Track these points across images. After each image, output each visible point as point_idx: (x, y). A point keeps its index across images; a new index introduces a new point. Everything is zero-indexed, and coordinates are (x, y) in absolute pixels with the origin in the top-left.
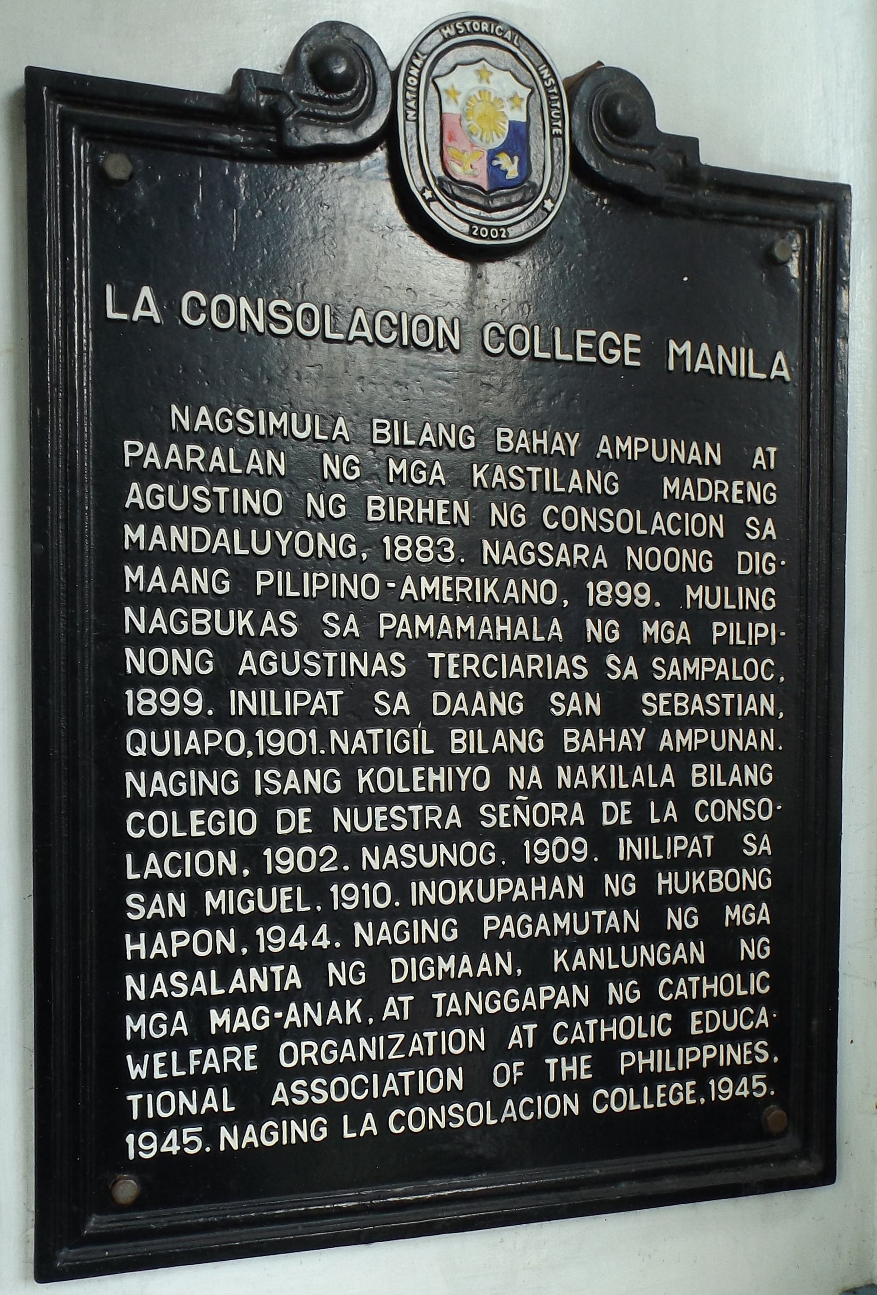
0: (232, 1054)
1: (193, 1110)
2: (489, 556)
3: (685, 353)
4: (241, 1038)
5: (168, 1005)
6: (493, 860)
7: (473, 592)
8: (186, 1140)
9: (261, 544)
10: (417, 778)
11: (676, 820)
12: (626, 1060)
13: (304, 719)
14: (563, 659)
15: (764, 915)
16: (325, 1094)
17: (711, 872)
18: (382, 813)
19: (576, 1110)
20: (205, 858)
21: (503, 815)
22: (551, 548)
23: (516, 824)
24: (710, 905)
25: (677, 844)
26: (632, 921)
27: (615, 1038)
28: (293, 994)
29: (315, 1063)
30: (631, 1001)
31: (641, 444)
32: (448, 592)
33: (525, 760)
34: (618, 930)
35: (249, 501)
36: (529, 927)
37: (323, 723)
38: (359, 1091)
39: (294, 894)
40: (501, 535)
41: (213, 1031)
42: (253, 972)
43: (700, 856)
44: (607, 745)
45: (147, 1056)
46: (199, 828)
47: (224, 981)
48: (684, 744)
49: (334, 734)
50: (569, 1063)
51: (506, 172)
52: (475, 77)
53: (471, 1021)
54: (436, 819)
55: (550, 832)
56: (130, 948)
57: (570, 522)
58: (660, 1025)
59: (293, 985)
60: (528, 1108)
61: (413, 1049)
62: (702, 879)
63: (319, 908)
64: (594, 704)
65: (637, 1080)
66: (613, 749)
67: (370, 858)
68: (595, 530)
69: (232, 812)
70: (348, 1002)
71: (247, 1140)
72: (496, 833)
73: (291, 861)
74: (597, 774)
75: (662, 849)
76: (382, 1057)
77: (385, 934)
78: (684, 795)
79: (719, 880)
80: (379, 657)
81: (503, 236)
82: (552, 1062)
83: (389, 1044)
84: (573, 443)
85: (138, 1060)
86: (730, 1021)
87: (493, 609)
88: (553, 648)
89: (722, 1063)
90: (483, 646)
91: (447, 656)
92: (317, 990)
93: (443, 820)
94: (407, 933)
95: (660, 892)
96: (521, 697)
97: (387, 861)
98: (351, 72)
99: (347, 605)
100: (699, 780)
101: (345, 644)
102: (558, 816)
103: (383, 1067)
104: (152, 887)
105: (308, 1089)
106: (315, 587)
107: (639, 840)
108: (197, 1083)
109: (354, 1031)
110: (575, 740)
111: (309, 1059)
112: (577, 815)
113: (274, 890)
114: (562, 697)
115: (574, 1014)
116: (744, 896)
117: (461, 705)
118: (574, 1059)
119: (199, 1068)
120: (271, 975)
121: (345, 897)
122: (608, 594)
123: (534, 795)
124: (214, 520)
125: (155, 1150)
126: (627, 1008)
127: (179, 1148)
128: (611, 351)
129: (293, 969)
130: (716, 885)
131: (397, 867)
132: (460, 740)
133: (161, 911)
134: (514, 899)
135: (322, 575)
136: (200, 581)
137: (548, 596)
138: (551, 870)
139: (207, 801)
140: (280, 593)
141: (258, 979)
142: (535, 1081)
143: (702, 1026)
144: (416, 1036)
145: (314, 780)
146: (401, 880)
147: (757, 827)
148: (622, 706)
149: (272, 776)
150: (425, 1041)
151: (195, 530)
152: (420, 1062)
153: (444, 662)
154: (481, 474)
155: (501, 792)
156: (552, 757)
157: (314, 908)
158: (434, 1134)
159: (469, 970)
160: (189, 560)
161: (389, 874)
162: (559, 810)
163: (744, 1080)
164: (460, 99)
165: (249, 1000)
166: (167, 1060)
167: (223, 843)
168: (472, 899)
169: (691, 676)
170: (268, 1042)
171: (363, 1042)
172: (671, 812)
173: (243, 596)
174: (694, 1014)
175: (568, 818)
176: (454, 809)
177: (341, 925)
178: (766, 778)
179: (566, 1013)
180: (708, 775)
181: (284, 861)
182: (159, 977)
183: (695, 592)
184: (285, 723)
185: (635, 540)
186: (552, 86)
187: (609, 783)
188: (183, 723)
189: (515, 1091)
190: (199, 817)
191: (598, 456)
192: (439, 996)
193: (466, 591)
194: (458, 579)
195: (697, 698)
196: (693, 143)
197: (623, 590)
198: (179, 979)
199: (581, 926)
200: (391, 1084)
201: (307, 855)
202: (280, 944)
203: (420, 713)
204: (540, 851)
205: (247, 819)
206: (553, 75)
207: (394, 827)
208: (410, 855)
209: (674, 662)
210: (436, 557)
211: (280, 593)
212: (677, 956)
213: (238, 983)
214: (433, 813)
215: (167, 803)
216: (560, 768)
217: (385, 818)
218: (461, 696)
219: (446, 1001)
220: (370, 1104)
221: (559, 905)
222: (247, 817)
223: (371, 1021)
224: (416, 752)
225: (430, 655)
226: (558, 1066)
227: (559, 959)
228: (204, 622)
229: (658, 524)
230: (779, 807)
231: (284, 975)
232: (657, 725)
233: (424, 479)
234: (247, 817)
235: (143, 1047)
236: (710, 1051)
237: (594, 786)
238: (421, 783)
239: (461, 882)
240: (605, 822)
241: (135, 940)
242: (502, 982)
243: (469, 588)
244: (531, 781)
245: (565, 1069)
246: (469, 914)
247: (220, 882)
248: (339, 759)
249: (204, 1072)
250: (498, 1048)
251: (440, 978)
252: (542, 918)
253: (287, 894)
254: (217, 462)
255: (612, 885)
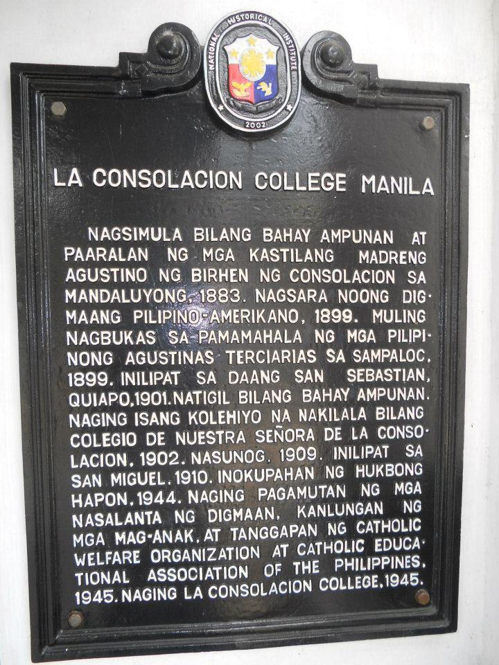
0: (127, 555)
2: (260, 298)
4: (132, 547)
5: (95, 530)
7: (250, 317)
9: (136, 297)
10: (220, 417)
11: (367, 438)
12: (339, 563)
14: (302, 352)
16: (175, 576)
17: (387, 465)
18: (202, 435)
21: (268, 436)
22: (295, 293)
24: (387, 483)
25: (368, 450)
27: (332, 552)
33: (282, 406)
34: (334, 496)
35: (129, 275)
36: (284, 494)
37: (169, 389)
39: (156, 475)
40: (266, 286)
41: (117, 543)
44: (327, 398)
45: (84, 555)
46: (107, 442)
47: (122, 518)
49: (175, 394)
50: (306, 564)
51: (265, 92)
55: (296, 444)
56: (74, 501)
57: (306, 277)
58: (358, 546)
61: (221, 556)
65: (345, 574)
70: (186, 531)
71: (135, 597)
73: (154, 459)
75: (358, 453)
76: (204, 560)
78: (372, 424)
79: (391, 470)
80: (199, 354)
81: (264, 126)
82: (297, 564)
83: (208, 554)
84: (306, 235)
86: (397, 544)
87: (261, 326)
88: (296, 346)
89: (392, 567)
90: (257, 346)
92: (169, 524)
93: (235, 439)
95: (357, 476)
96: (278, 373)
97: (205, 460)
100: (380, 416)
101: (181, 347)
103: (205, 565)
104: (84, 471)
105: (166, 573)
106: (165, 318)
108: (111, 568)
109: (190, 546)
111: (166, 559)
112: (311, 435)
114: (302, 372)
115: (310, 540)
116: (405, 479)
117: (244, 378)
118: (309, 562)
119: (110, 561)
120: (146, 517)
122: (327, 316)
123: (286, 424)
124: (111, 286)
126: (339, 537)
128: (328, 184)
129: (157, 513)
133: (89, 483)
136: (105, 317)
138: (295, 465)
139: (111, 429)
141: (139, 518)
142: (288, 573)
144: (222, 550)
145: (165, 418)
147: (414, 441)
148: (336, 376)
149: (144, 416)
151: (102, 291)
153: (235, 356)
154: (254, 254)
155: (267, 424)
157: (167, 483)
159: (250, 516)
160: (99, 307)
161: (206, 466)
163: (406, 576)
165: (136, 528)
166: (95, 557)
167: (120, 450)
168: (252, 480)
170: (146, 549)
173: (127, 324)
175: (305, 437)
177: (181, 491)
179: (303, 538)
180: (386, 413)
182: (89, 516)
184: (150, 389)
185: (343, 286)
186: (291, 44)
187: (328, 418)
188: (98, 389)
189: (276, 579)
190: (107, 437)
192: (234, 530)
194: (242, 311)
196: (374, 68)
199: (313, 493)
204: (291, 455)
207: (208, 442)
208: (217, 457)
210: (229, 299)
212: (367, 510)
213: (129, 519)
216: (301, 411)
218: (245, 373)
219: (238, 533)
220: (198, 582)
225: (227, 352)
226: (300, 567)
227: (300, 511)
228: (107, 338)
229: (357, 277)
231: (152, 516)
232: (356, 387)
233: (222, 259)
235: (82, 550)
237: (320, 420)
238: (222, 420)
240: (326, 439)
241: (77, 498)
242: (269, 523)
243: (249, 315)
244: (284, 418)
245: (304, 568)
246: (250, 489)
247: (118, 469)
248: (178, 407)
249: (113, 563)
250: (267, 556)
251: (235, 520)
252: (291, 489)
255: (330, 472)
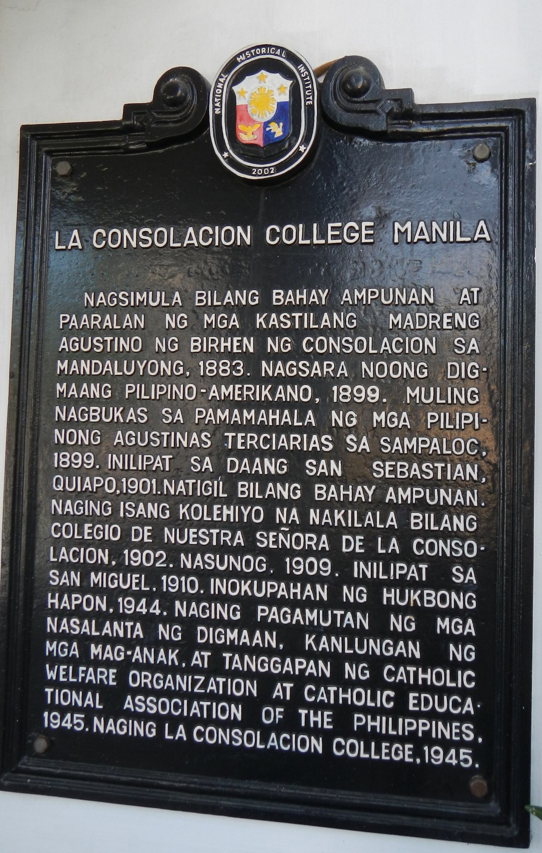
0: (102, 673)
1: (80, 703)
2: (266, 371)
3: (407, 230)
4: (108, 664)
5: (69, 638)
6: (264, 569)
7: (254, 394)
8: (75, 721)
9: (129, 369)
10: (216, 512)
11: (398, 552)
12: (359, 720)
13: (148, 472)
14: (315, 437)
15: (470, 628)
16: (154, 707)
17: (426, 592)
18: (194, 533)
19: (320, 750)
20: (91, 553)
21: (271, 539)
22: (308, 365)
23: (280, 547)
24: (426, 617)
25: (399, 569)
26: (363, 621)
27: (349, 702)
28: (138, 641)
29: (150, 686)
30: (362, 678)
31: (373, 293)
32: (239, 395)
33: (288, 504)
34: (353, 626)
35: (123, 343)
36: (289, 616)
37: (158, 475)
38: (176, 709)
39: (140, 578)
40: (274, 357)
41: (92, 657)
42: (116, 624)
43: (417, 579)
44: (346, 496)
45: (56, 667)
46: (89, 534)
47: (99, 628)
48: (405, 498)
49: (166, 482)
50: (316, 715)
51: (275, 133)
52: (257, 81)
53: (248, 675)
54: (227, 539)
55: (306, 553)
56: (50, 601)
57: (321, 347)
58: (385, 698)
59: (138, 636)
60: (286, 742)
61: (210, 688)
62: (419, 596)
63: (154, 589)
64: (336, 468)
65: (367, 736)
66: (350, 499)
67: (186, 561)
68: (339, 351)
69: (107, 526)
70: (170, 651)
71: (109, 728)
72: (266, 551)
73: (139, 558)
74: (338, 516)
75: (386, 571)
76: (190, 690)
77: (194, 610)
78: (405, 535)
79: (432, 598)
80: (195, 435)
81: (272, 172)
82: (303, 712)
83: (195, 682)
84: (323, 296)
85: (52, 668)
86: (441, 704)
87: (267, 405)
88: (308, 430)
89: (434, 735)
90: (261, 428)
91: (237, 435)
92: (152, 641)
93: (232, 540)
94: (208, 611)
95: (385, 602)
96: (286, 462)
97: (196, 564)
98: (183, 94)
99: (174, 403)
100: (416, 524)
101: (174, 426)
102: (310, 543)
103: (191, 697)
104: (62, 566)
105: (145, 702)
106: (159, 393)
107: (370, 564)
108: (83, 687)
109: (173, 670)
110: (323, 492)
111: (145, 684)
112: (324, 543)
113: (129, 575)
114: (314, 462)
115: (321, 681)
116: (452, 612)
117: (245, 466)
118: (320, 713)
119: (84, 679)
120: (125, 628)
121: (170, 583)
122: (348, 394)
123: (293, 527)
124: (103, 356)
125: (59, 724)
126: (358, 683)
127: (71, 725)
128: (352, 235)
129: (138, 625)
130: (429, 602)
131: (202, 568)
132: (245, 489)
133: (67, 581)
134: (279, 597)
135: (163, 385)
136: (95, 391)
137: (305, 396)
138: (304, 579)
139: (94, 519)
140: (138, 397)
141: (118, 629)
142: (290, 723)
143: (418, 705)
144: (212, 679)
145: (153, 510)
146: (205, 576)
147: (465, 562)
148: (357, 471)
149: (130, 506)
150: (217, 684)
151: (94, 362)
152: (213, 697)
153: (235, 438)
154: (261, 320)
155: (270, 524)
156: (306, 503)
157: (151, 589)
158: (220, 748)
159: (247, 641)
160: (90, 379)
161: (196, 572)
162: (311, 539)
163: (453, 752)
164: (247, 96)
165: (114, 641)
166: (67, 670)
167: (102, 544)
168: (250, 594)
169: (410, 451)
170: (124, 668)
171: (178, 678)
172: (394, 546)
173: (118, 400)
174: (411, 695)
175: (317, 544)
176: (239, 533)
177: (168, 601)
178: (471, 525)
179: (312, 679)
180: (423, 521)
181: (135, 558)
182: (65, 621)
183: (413, 391)
184: (139, 473)
185: (368, 357)
186: (306, 77)
187: (346, 522)
188: (82, 472)
189: (278, 728)
190: (89, 528)
191: (342, 303)
192: (227, 655)
193: (250, 393)
194: (245, 386)
195: (415, 466)
196: (408, 92)
197: (359, 391)
198: (75, 623)
199: (325, 619)
200: (195, 709)
201: (148, 555)
202: (131, 609)
203: (219, 472)
204: (298, 566)
205: (115, 531)
206: (308, 70)
207: (201, 542)
208: (211, 561)
209: (397, 440)
210: (231, 373)
211: (138, 397)
212: (398, 651)
213: (107, 630)
214: (226, 535)
215: (73, 518)
216: (312, 511)
217: (195, 536)
218: (246, 460)
219: (231, 659)
220: (181, 719)
221: (308, 604)
222: (115, 530)
223: (184, 665)
224: (215, 495)
225: (226, 434)
226: (307, 716)
227: (309, 641)
228: (96, 414)
229: (386, 346)
230: (482, 548)
231: (133, 628)
232: (385, 483)
233: (225, 325)
234: (115, 530)
235: (55, 661)
236: (424, 725)
237: (336, 524)
238: (218, 516)
239: (243, 582)
240: (344, 550)
241: (53, 597)
242: (270, 652)
243: (253, 391)
244: (291, 518)
245: (312, 719)
246: (248, 604)
247: (98, 567)
248: (168, 497)
249: (87, 681)
250: (265, 696)
251: (228, 643)
252: (298, 611)
253: (136, 578)
254: (107, 323)
255: (348, 593)
